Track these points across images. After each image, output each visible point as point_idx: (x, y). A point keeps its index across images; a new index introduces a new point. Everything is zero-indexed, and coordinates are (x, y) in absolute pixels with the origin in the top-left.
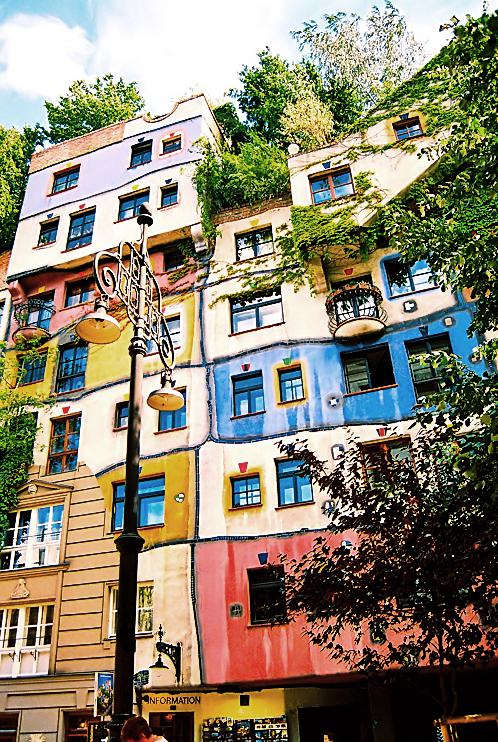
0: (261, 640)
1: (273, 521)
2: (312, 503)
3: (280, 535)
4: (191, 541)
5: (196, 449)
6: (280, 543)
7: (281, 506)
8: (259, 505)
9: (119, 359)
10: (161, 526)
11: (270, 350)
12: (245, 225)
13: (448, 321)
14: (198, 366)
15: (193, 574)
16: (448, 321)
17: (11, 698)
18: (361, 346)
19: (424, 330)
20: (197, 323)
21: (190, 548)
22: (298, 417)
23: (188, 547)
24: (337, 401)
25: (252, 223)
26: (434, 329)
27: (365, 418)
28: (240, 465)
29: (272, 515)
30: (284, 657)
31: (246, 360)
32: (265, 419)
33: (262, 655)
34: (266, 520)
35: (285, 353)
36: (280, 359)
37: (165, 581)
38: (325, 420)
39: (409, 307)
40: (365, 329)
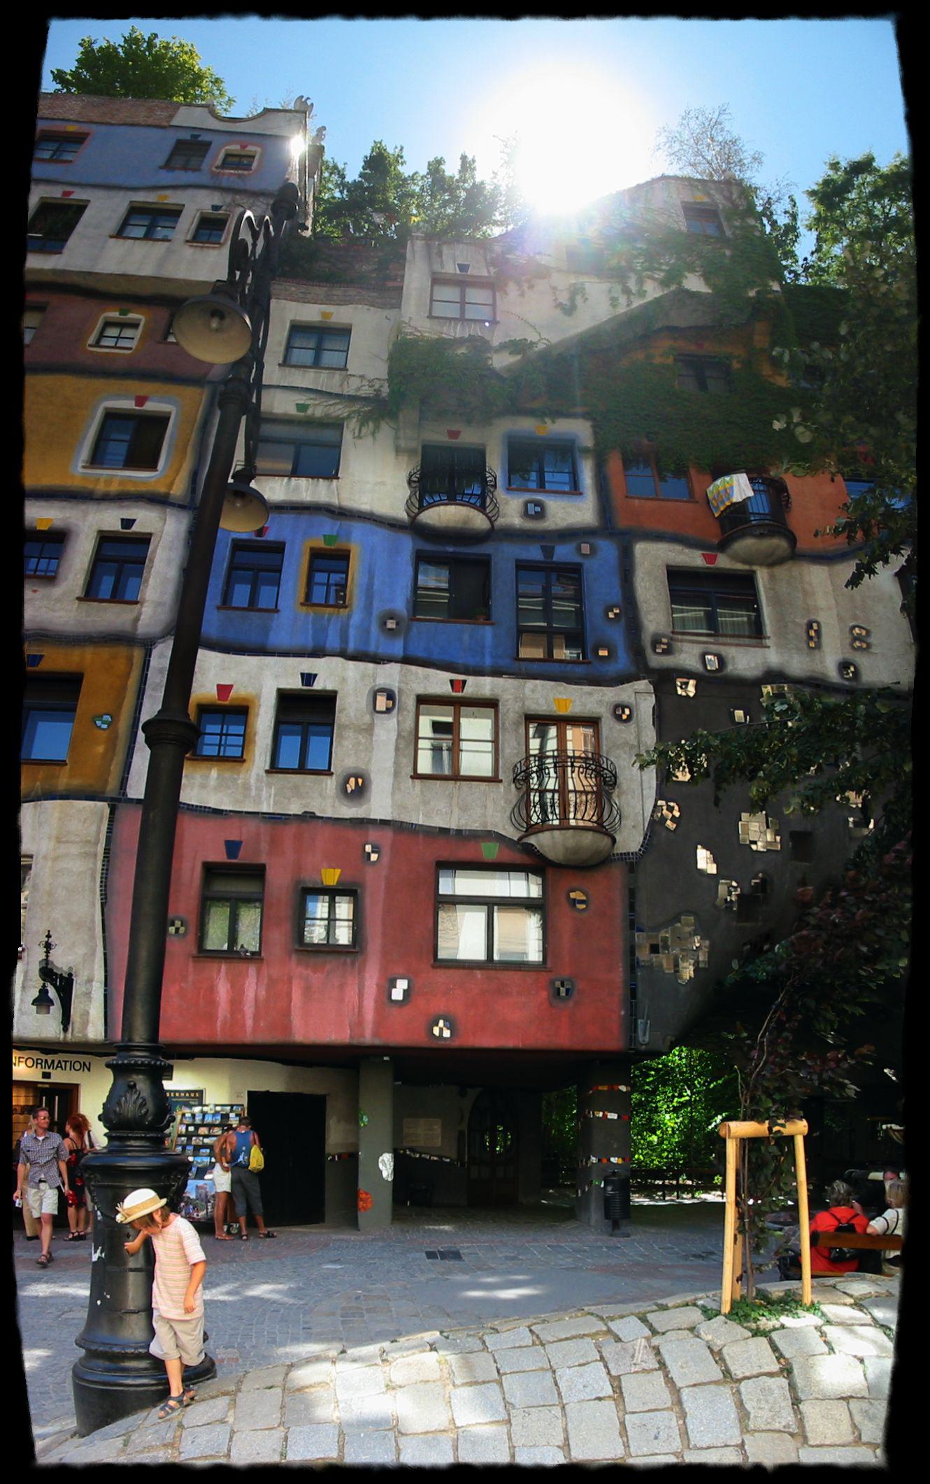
1: (259, 789)
2: (328, 772)
4: (112, 799)
6: (264, 828)
7: (274, 768)
8: (240, 760)
10: (62, 763)
11: (305, 518)
13: (586, 548)
14: (181, 507)
15: (107, 851)
16: (586, 548)
18: (451, 549)
19: (548, 551)
21: (107, 811)
22: (330, 632)
23: (103, 807)
24: (397, 624)
26: (563, 553)
28: (220, 687)
29: (259, 779)
34: (246, 787)
35: (328, 526)
36: (320, 534)
37: (56, 859)
38: (372, 648)
39: (532, 509)
40: (466, 522)
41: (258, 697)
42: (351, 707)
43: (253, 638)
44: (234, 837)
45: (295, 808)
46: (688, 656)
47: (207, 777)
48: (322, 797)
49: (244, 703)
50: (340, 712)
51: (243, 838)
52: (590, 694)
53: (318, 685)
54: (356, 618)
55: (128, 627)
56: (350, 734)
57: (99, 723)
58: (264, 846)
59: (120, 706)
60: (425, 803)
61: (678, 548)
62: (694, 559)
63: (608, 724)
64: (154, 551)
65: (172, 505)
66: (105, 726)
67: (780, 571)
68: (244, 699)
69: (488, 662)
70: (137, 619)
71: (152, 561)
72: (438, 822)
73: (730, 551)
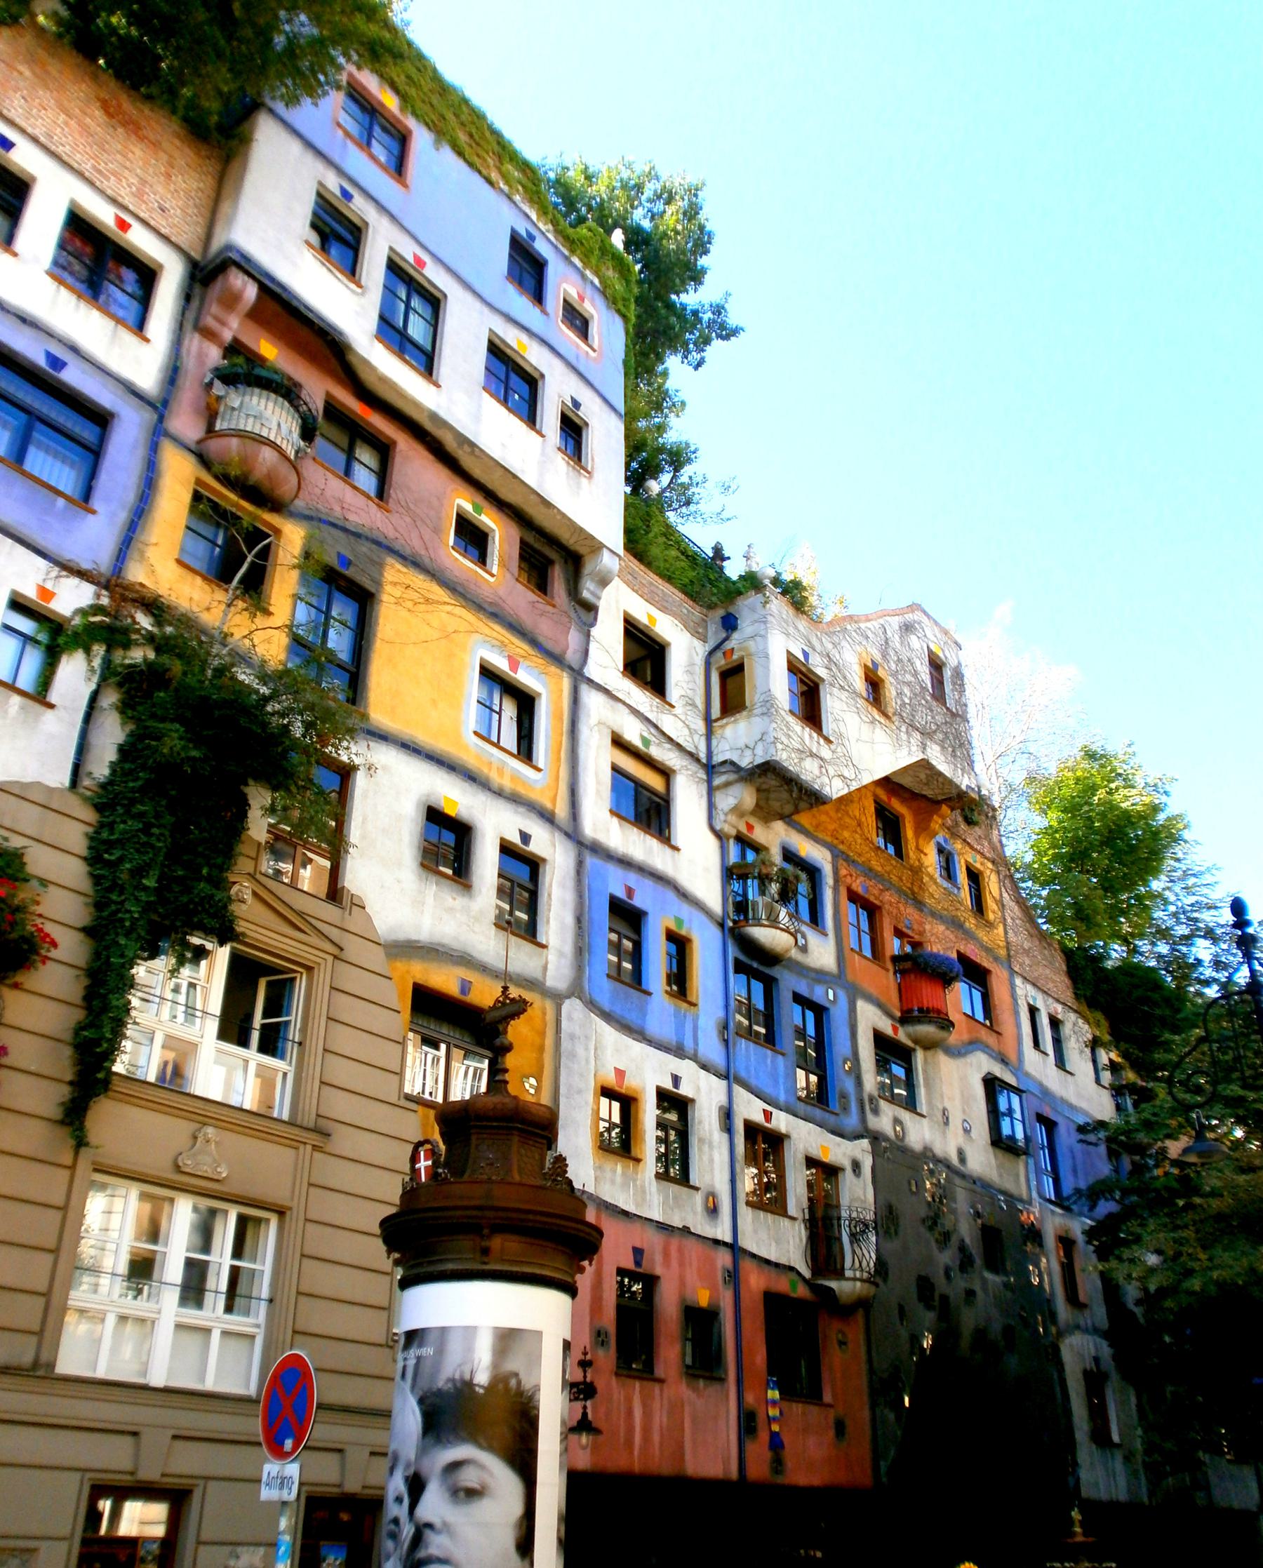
0: (629, 1400)
3: (662, 1227)
5: (559, 999)
9: (434, 703)
11: (659, 887)
12: (643, 612)
13: (831, 992)
14: (567, 834)
16: (831, 992)
17: (180, 1444)
18: (755, 965)
20: (565, 739)
25: (650, 617)
27: (753, 1082)
30: (656, 1437)
31: (633, 879)
32: (649, 1007)
33: (630, 1430)
34: (644, 1192)
41: (644, 1088)
42: (706, 1119)
43: (632, 1018)
44: (638, 1245)
45: (677, 1222)
46: (885, 1120)
47: (615, 1171)
48: (690, 1214)
49: (634, 1095)
50: (700, 1122)
51: (645, 1247)
52: (839, 1145)
53: (685, 1090)
54: (702, 1022)
55: (537, 974)
56: (706, 1148)
57: (527, 1086)
58: (658, 1258)
59: (542, 1071)
60: (755, 1231)
61: (879, 1012)
62: (886, 1026)
63: (848, 1178)
64: (551, 885)
65: (559, 828)
66: (532, 1091)
67: (929, 1053)
68: (635, 1090)
69: (782, 1098)
70: (545, 968)
71: (549, 895)
72: (764, 1253)
73: (911, 1029)
